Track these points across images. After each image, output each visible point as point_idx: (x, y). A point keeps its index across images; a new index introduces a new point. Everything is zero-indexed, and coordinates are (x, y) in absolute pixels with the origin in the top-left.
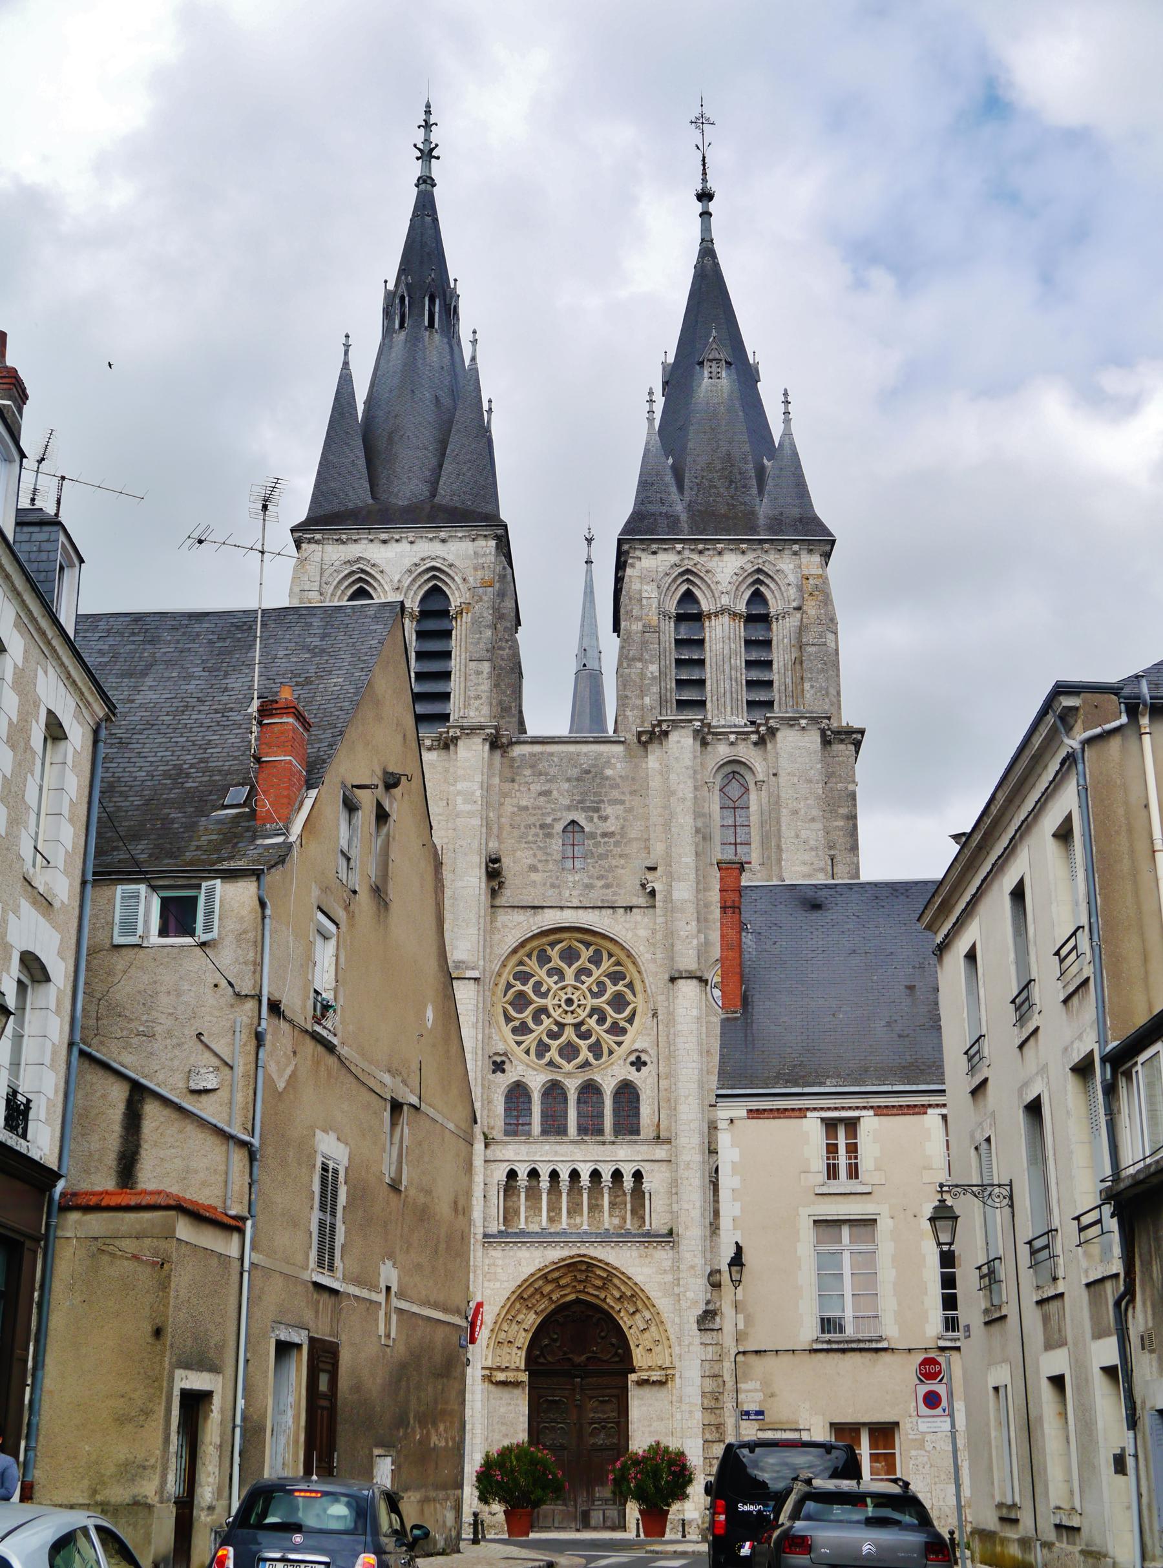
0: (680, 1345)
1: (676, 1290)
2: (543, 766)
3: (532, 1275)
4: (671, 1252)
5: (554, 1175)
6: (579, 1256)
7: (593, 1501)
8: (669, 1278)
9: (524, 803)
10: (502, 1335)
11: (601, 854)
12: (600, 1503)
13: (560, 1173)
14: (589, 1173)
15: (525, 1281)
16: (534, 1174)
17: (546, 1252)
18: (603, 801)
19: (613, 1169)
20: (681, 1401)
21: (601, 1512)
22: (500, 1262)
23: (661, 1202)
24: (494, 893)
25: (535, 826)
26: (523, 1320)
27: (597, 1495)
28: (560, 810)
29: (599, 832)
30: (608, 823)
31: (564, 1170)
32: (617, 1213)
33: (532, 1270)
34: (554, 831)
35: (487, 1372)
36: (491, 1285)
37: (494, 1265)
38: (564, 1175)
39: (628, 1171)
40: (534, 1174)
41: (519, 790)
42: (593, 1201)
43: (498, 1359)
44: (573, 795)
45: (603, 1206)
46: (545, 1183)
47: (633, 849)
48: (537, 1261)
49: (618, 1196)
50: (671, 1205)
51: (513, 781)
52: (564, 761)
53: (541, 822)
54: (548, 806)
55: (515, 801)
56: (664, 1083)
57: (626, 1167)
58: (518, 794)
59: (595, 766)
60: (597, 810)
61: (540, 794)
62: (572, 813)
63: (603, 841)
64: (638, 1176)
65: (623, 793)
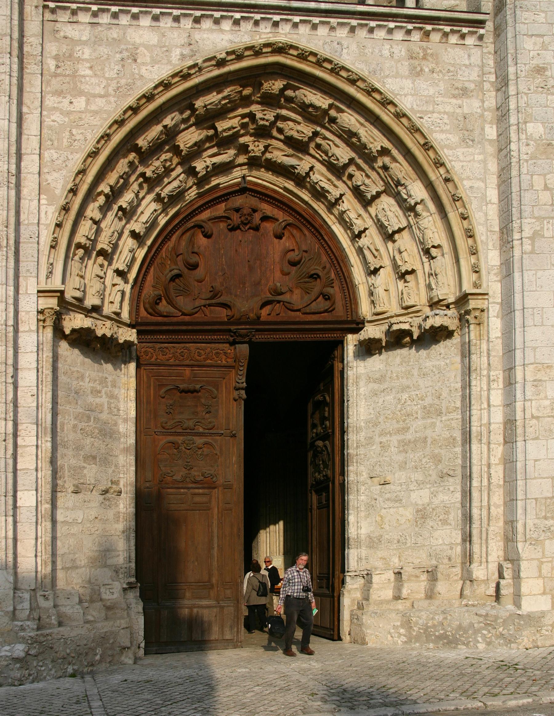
4: (476, 53)
15: (149, 97)
17: (197, 36)
22: (87, 53)
48: (176, 53)
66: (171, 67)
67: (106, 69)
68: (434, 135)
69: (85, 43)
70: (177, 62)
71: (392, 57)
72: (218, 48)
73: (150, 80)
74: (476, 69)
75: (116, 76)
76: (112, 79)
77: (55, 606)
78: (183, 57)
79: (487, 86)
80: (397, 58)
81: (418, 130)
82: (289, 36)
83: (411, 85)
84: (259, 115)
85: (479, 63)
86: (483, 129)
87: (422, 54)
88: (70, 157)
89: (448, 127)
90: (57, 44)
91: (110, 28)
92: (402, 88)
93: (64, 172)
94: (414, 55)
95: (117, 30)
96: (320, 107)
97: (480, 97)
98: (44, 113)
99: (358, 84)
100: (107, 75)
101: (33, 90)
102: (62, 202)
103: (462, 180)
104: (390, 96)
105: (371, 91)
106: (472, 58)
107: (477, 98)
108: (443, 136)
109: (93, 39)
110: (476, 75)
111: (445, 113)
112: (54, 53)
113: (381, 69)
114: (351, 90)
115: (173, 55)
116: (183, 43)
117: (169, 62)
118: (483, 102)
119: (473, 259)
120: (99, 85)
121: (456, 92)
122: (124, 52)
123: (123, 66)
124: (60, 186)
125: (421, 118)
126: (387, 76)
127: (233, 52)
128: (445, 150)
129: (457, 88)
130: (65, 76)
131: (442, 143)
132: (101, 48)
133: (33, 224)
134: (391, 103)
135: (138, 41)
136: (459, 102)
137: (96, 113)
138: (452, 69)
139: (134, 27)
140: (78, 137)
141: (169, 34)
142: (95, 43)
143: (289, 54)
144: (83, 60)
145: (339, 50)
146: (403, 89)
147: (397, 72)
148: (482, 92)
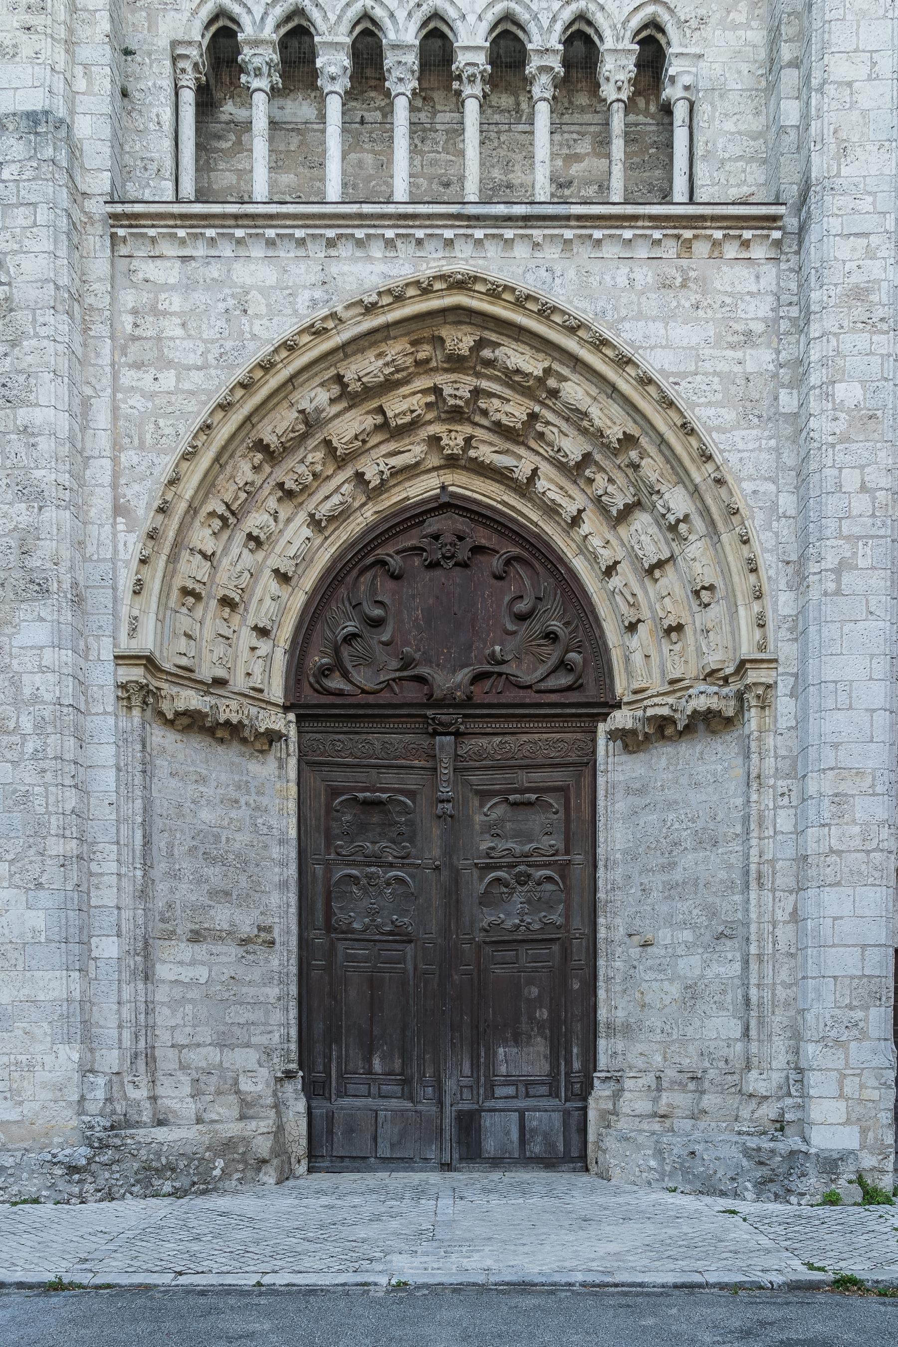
3: (289, 346)
7: (491, 1087)
12: (511, 1090)
13: (387, 23)
15: (267, 367)
21: (515, 1116)
22: (176, 302)
27: (503, 1069)
31: (401, 15)
35: (137, 674)
36: (146, 380)
37: (156, 312)
48: (303, 298)
66: (297, 320)
67: (204, 326)
68: (697, 409)
69: (173, 288)
70: (306, 312)
71: (632, 287)
72: (366, 286)
73: (268, 341)
74: (770, 299)
75: (218, 336)
76: (213, 342)
78: (314, 303)
79: (784, 325)
80: (640, 288)
81: (671, 404)
82: (471, 262)
83: (663, 331)
84: (447, 391)
85: (774, 288)
86: (776, 398)
87: (679, 280)
88: (156, 462)
89: (719, 396)
90: (133, 291)
91: (208, 263)
92: (646, 337)
93: (148, 484)
94: (667, 282)
95: (219, 266)
96: (531, 374)
97: (774, 345)
98: (120, 396)
99: (580, 333)
100: (205, 336)
101: (100, 362)
102: (146, 527)
103: (740, 480)
104: (628, 351)
105: (600, 343)
106: (761, 280)
107: (769, 346)
108: (711, 412)
109: (185, 281)
110: (768, 308)
111: (715, 373)
112: (130, 305)
113: (615, 308)
114: (570, 344)
115: (299, 300)
116: (313, 281)
117: (296, 311)
118: (778, 352)
119: (756, 607)
120: (194, 351)
121: (736, 338)
122: (229, 299)
123: (228, 321)
124: (142, 504)
125: (675, 384)
126: (624, 319)
127: (389, 292)
128: (714, 435)
129: (736, 332)
130: (146, 338)
131: (709, 423)
132: (196, 295)
133: (104, 560)
134: (629, 361)
135: (248, 281)
136: (739, 354)
137: (192, 393)
138: (728, 300)
139: (242, 260)
140: (166, 431)
141: (292, 268)
142: (187, 287)
143: (474, 291)
144: (171, 314)
145: (549, 280)
146: (648, 337)
147: (640, 312)
148: (778, 337)
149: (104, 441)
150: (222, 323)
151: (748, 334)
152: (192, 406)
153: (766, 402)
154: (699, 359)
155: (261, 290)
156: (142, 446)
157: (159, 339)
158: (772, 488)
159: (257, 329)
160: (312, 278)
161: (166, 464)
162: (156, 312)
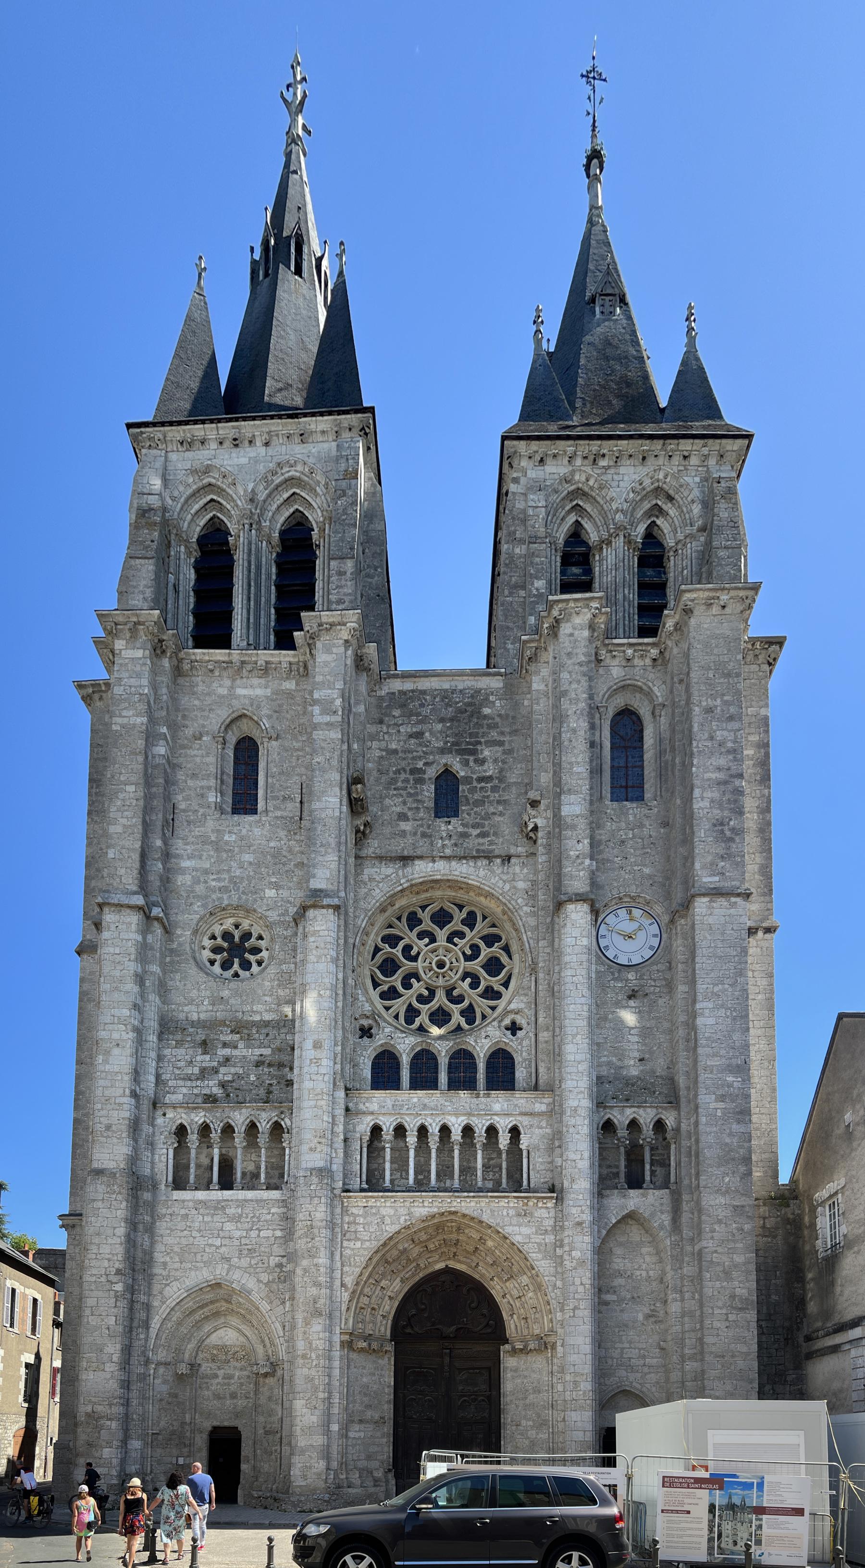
0: (562, 1310)
1: (559, 1252)
2: (413, 705)
5: (423, 1131)
6: (451, 1213)
8: (550, 1238)
9: (394, 746)
10: (365, 1300)
11: (476, 800)
14: (460, 1128)
16: (400, 1131)
18: (480, 743)
19: (487, 1124)
20: (562, 1370)
23: (540, 1160)
24: (361, 836)
25: (405, 771)
26: (389, 1287)
28: (432, 753)
29: (475, 777)
30: (485, 767)
31: (434, 1125)
32: (491, 1177)
33: (396, 1228)
34: (426, 776)
35: (346, 1338)
36: (351, 1244)
37: (354, 1223)
38: (434, 1129)
39: (503, 1124)
40: (400, 1131)
41: (387, 733)
42: (465, 1163)
43: (360, 1325)
44: (447, 736)
45: (475, 1169)
46: (412, 1139)
47: (511, 795)
49: (492, 1159)
50: (551, 1162)
51: (381, 722)
52: (437, 699)
53: (411, 766)
54: (419, 749)
55: (383, 744)
56: (544, 1036)
57: (502, 1121)
58: (386, 737)
59: (470, 704)
60: (473, 752)
61: (411, 736)
62: (446, 756)
63: (479, 786)
64: (515, 1132)
65: (502, 733)
77: (347, 1478)
78: (406, 1221)
81: (521, 1252)
102: (351, 1290)
104: (507, 1235)
135: (385, 1213)
149: (339, 1264)
150: (376, 1226)
151: (546, 1230)
152: (366, 1253)
153: (552, 1252)
154: (530, 1238)
155: (390, 1217)
156: (350, 1265)
157: (355, 1232)
158: (554, 1279)
159: (387, 1228)
160: (405, 1213)
161: (358, 1270)
162: (354, 1223)
